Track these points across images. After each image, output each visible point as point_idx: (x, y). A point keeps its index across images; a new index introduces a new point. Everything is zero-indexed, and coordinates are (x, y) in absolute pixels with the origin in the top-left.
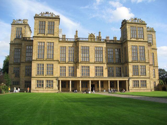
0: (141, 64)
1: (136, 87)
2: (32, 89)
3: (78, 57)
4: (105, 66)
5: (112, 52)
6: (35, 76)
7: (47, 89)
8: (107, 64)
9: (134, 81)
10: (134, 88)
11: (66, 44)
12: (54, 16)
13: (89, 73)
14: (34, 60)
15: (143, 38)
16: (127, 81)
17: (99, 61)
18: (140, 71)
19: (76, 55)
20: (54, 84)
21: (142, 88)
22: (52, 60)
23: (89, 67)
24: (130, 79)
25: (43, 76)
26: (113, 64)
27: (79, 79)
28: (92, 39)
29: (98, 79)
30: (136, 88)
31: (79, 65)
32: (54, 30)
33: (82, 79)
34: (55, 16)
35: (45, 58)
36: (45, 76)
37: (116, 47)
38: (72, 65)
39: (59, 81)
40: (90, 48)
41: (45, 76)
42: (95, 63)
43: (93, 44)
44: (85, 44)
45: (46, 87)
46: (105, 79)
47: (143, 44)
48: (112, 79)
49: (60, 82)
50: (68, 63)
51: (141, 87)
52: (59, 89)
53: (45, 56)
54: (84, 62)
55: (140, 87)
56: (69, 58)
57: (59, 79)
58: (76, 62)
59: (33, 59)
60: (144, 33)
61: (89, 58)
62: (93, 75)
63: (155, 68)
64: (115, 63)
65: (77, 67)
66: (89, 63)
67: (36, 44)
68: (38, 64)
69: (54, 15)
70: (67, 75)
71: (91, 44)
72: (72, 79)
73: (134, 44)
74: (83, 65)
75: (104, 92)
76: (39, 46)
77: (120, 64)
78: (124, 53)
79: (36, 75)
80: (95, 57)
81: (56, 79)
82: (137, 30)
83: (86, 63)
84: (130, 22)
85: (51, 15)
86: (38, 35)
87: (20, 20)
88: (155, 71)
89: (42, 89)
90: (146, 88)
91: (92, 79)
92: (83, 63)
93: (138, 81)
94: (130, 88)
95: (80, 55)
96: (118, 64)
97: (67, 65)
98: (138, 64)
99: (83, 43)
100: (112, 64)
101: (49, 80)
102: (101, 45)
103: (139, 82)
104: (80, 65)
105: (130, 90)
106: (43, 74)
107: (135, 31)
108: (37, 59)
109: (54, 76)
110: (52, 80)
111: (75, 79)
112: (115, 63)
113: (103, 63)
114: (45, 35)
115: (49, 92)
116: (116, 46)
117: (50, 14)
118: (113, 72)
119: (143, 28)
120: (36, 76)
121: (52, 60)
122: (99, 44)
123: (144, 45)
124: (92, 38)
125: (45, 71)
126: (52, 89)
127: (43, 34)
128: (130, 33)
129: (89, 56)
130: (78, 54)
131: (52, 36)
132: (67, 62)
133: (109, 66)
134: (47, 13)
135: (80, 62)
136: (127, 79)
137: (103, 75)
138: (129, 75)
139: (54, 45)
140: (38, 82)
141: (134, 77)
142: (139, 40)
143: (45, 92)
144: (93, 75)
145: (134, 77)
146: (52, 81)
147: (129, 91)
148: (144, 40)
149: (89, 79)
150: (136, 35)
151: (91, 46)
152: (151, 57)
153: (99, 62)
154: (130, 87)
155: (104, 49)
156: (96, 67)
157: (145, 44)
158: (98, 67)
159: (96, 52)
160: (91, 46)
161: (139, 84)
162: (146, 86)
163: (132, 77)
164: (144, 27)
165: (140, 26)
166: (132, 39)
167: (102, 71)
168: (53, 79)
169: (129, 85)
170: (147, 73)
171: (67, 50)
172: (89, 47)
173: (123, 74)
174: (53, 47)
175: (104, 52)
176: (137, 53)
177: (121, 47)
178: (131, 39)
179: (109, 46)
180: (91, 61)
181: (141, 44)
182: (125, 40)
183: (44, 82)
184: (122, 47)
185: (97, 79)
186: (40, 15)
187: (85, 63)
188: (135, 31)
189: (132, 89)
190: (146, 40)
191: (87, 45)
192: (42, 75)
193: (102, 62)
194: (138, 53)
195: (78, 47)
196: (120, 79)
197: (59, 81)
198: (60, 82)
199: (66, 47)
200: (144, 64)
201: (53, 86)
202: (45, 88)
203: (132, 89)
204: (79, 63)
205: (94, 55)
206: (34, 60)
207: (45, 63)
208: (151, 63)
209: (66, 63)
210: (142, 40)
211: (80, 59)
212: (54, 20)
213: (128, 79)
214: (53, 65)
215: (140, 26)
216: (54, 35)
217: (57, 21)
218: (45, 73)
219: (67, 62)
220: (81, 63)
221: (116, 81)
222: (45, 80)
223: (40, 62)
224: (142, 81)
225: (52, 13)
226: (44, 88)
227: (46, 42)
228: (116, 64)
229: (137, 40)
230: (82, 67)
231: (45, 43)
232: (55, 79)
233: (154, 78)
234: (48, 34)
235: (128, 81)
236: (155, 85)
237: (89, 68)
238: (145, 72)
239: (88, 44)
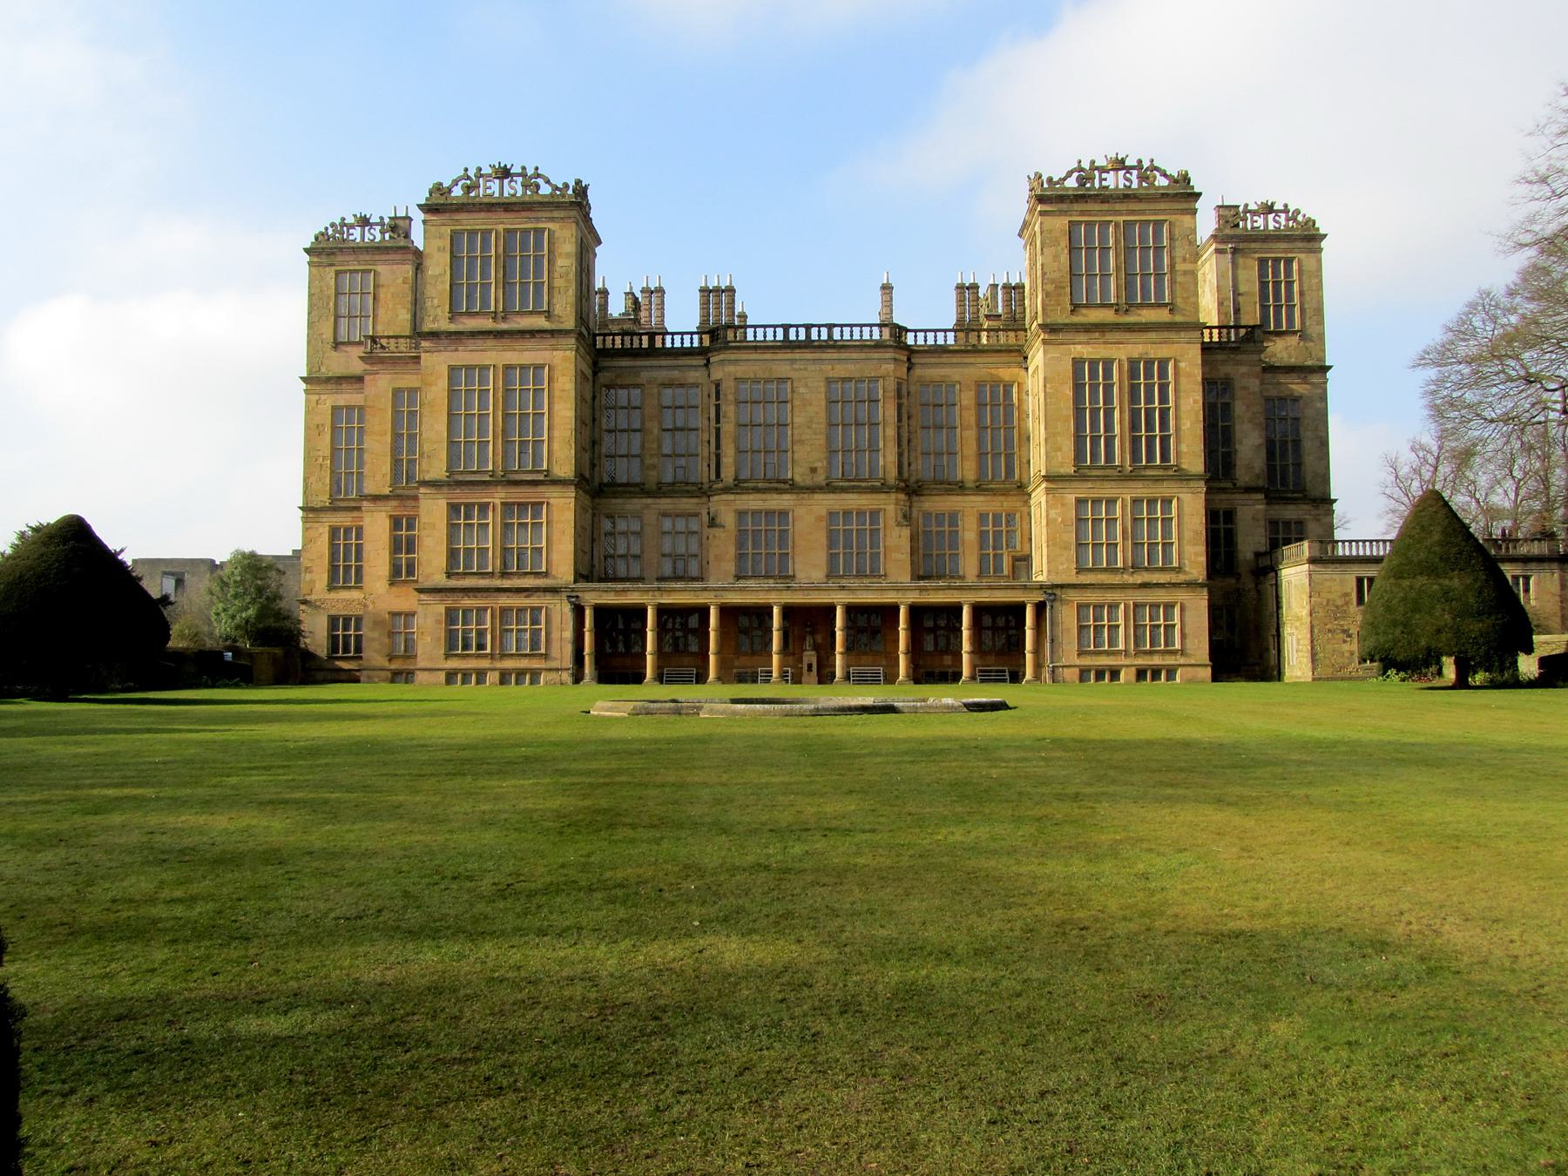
12: (545, 190)
34: (557, 188)
42: (829, 488)
49: (588, 614)
69: (548, 182)
74: (752, 502)
75: (901, 683)
85: (525, 186)
87: (364, 222)
117: (520, 179)
131: (541, 322)
134: (504, 173)
148: (1178, 318)
186: (457, 192)
198: (588, 614)
225: (530, 172)
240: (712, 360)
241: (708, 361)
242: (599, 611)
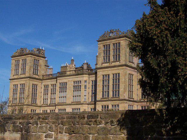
43: (72, 78)
47: (118, 69)
50: (49, 106)
71: (69, 78)
74: (60, 107)
92: (59, 105)
99: (61, 78)
122: (77, 77)
132: (48, 105)
142: (113, 64)
153: (77, 102)
164: (121, 42)
165: (116, 41)
181: (115, 71)
190: (124, 63)
191: (65, 81)
209: (47, 106)
210: (117, 63)
212: (27, 57)
215: (116, 41)
217: (28, 57)
239: (65, 79)
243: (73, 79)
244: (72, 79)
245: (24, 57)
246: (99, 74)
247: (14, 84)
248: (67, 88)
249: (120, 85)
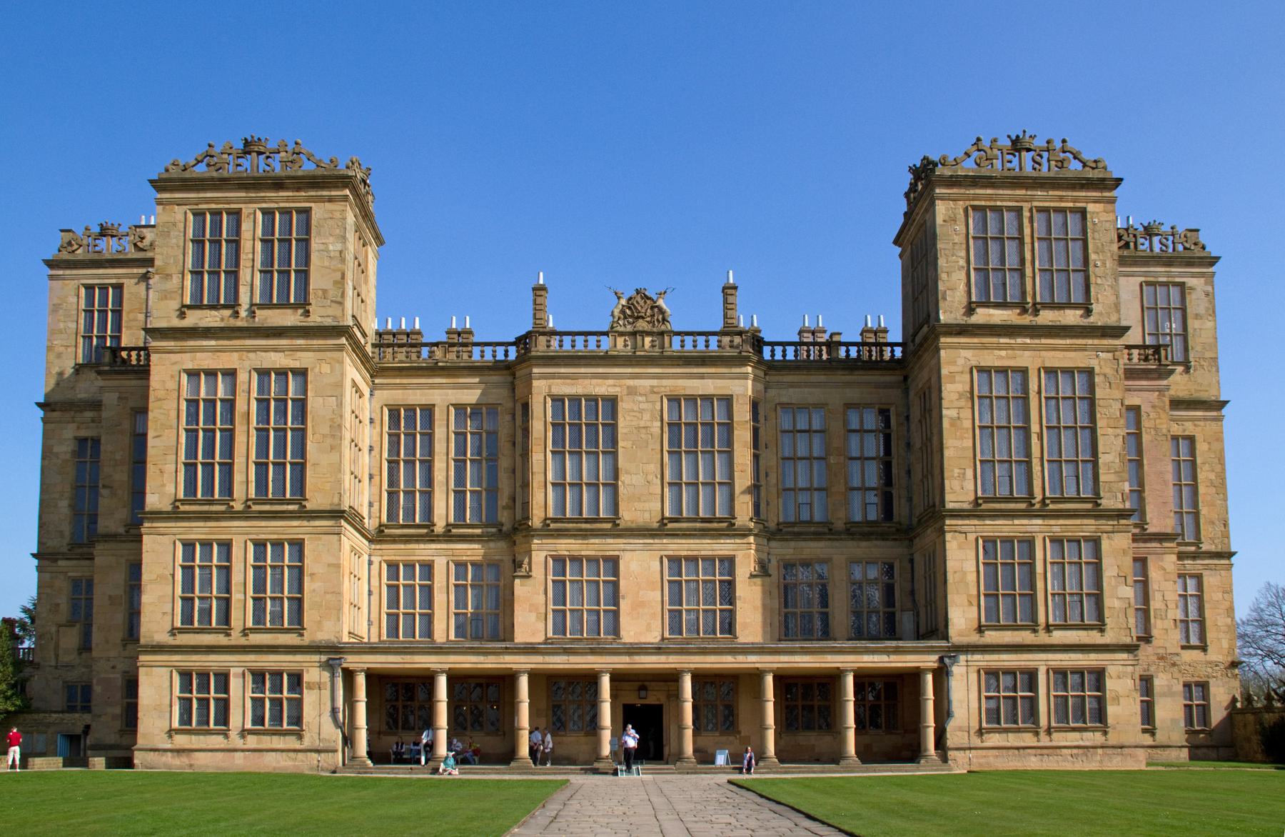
0: (1058, 527)
1: (1006, 731)
2: (141, 742)
3: (526, 485)
4: (746, 555)
5: (817, 440)
6: (163, 637)
7: (252, 741)
8: (770, 533)
9: (993, 673)
10: (994, 739)
11: (432, 386)
13: (616, 615)
14: (158, 516)
15: (1077, 297)
16: (929, 677)
17: (701, 515)
18: (1046, 584)
19: (514, 471)
20: (309, 698)
21: (1060, 739)
22: (291, 507)
23: (614, 562)
24: (954, 659)
25: (220, 639)
26: (826, 531)
27: (508, 658)
28: (645, 333)
29: (672, 658)
30: (1013, 740)
31: (529, 553)
32: (304, 275)
33: (539, 659)
35: (238, 491)
36: (236, 638)
37: (853, 394)
38: (473, 551)
39: (349, 676)
40: (622, 406)
41: (243, 641)
44: (585, 376)
45: (249, 725)
46: (729, 658)
47: (1083, 349)
48: (797, 658)
49: (361, 680)
51: (1059, 730)
52: (348, 740)
53: (238, 478)
54: (570, 521)
55: (1043, 721)
56: (460, 495)
57: (351, 661)
58: (515, 529)
59: (155, 499)
60: (1093, 257)
61: (613, 488)
62: (649, 628)
63: (1207, 567)
64: (839, 525)
65: (517, 565)
66: (617, 530)
67: (172, 385)
68: (189, 546)
70: (443, 629)
72: (452, 658)
73: (999, 355)
74: (566, 546)
76: (193, 403)
77: (883, 536)
78: (917, 443)
79: (174, 631)
80: (667, 479)
81: (324, 658)
82: (1027, 231)
83: (585, 528)
84: (968, 167)
86: (182, 315)
88: (1200, 587)
89: (217, 741)
90: (1097, 738)
91: (622, 662)
92: (560, 534)
93: (1031, 675)
94: (954, 737)
95: (542, 463)
96: (866, 536)
97: (441, 557)
98: (1034, 526)
100: (817, 536)
101: (274, 666)
102: (719, 383)
103: (1032, 684)
104: (540, 553)
105: (951, 754)
106: (226, 617)
107: (1011, 248)
108: (182, 508)
109: (307, 639)
110: (294, 667)
111: (481, 658)
112: (839, 525)
113: (729, 529)
114: (236, 314)
115: (272, 762)
116: (848, 384)
118: (824, 601)
119: (1083, 213)
120: (170, 640)
121: (291, 507)
122: (702, 376)
123: (1093, 363)
124: (642, 325)
125: (236, 596)
126: (291, 742)
127: (225, 307)
128: (962, 263)
129: (616, 477)
130: (526, 454)
132: (440, 527)
133: (787, 550)
135: (536, 522)
136: (930, 661)
137: (729, 627)
138: (946, 626)
139: (305, 392)
140: (186, 687)
141: (992, 637)
143: (239, 762)
144: (649, 628)
145: (992, 637)
146: (297, 680)
147: (945, 759)
148: (1094, 320)
149: (591, 658)
150: (1023, 276)
151: (632, 391)
152: (1159, 470)
153: (704, 520)
154: (951, 726)
155: (742, 414)
156: (675, 561)
157: (1097, 349)
158: (693, 560)
159: (675, 441)
160: (632, 391)
161: (1033, 703)
162: (1100, 715)
163: (974, 639)
166: (983, 316)
167: (729, 590)
168: (299, 658)
169: (943, 713)
170: (1108, 602)
171: (439, 432)
172: (612, 403)
173: (906, 621)
174: (301, 405)
175: (743, 436)
176: (1026, 430)
177: (895, 394)
178: (970, 310)
179: (792, 385)
180: (629, 515)
182: (925, 329)
183: (235, 684)
184: (906, 391)
185: (663, 658)
187: (584, 535)
188: (1011, 248)
189: (976, 741)
191: (602, 388)
192: (216, 631)
193: (720, 520)
194: (1035, 428)
195: (526, 407)
196: (866, 658)
197: (349, 676)
199: (429, 410)
200: (1087, 527)
201: (297, 719)
202: (244, 733)
203: (976, 741)
204: (529, 533)
205: (654, 468)
206: (158, 516)
207: (241, 535)
208: (1160, 518)
209: (432, 538)
210: (1072, 317)
211: (542, 503)
213: (941, 660)
214: (298, 545)
216: (307, 314)
218: (242, 614)
219: (440, 527)
220: (552, 529)
221: (831, 680)
222: (237, 666)
223: (199, 530)
224: (1061, 674)
226: (233, 734)
227: (247, 365)
228: (854, 531)
229: (1027, 320)
230: (560, 561)
231: (242, 377)
232: (316, 658)
233: (1196, 655)
234: (262, 306)
235: (941, 675)
236: (1205, 710)
237: (616, 572)
238: (1098, 599)
240: (518, 374)
241: (514, 375)
242: (375, 678)
243: (665, 382)
244: (655, 382)
245: (288, 200)
246: (954, 363)
247: (190, 366)
248: (622, 430)
249: (1099, 432)
